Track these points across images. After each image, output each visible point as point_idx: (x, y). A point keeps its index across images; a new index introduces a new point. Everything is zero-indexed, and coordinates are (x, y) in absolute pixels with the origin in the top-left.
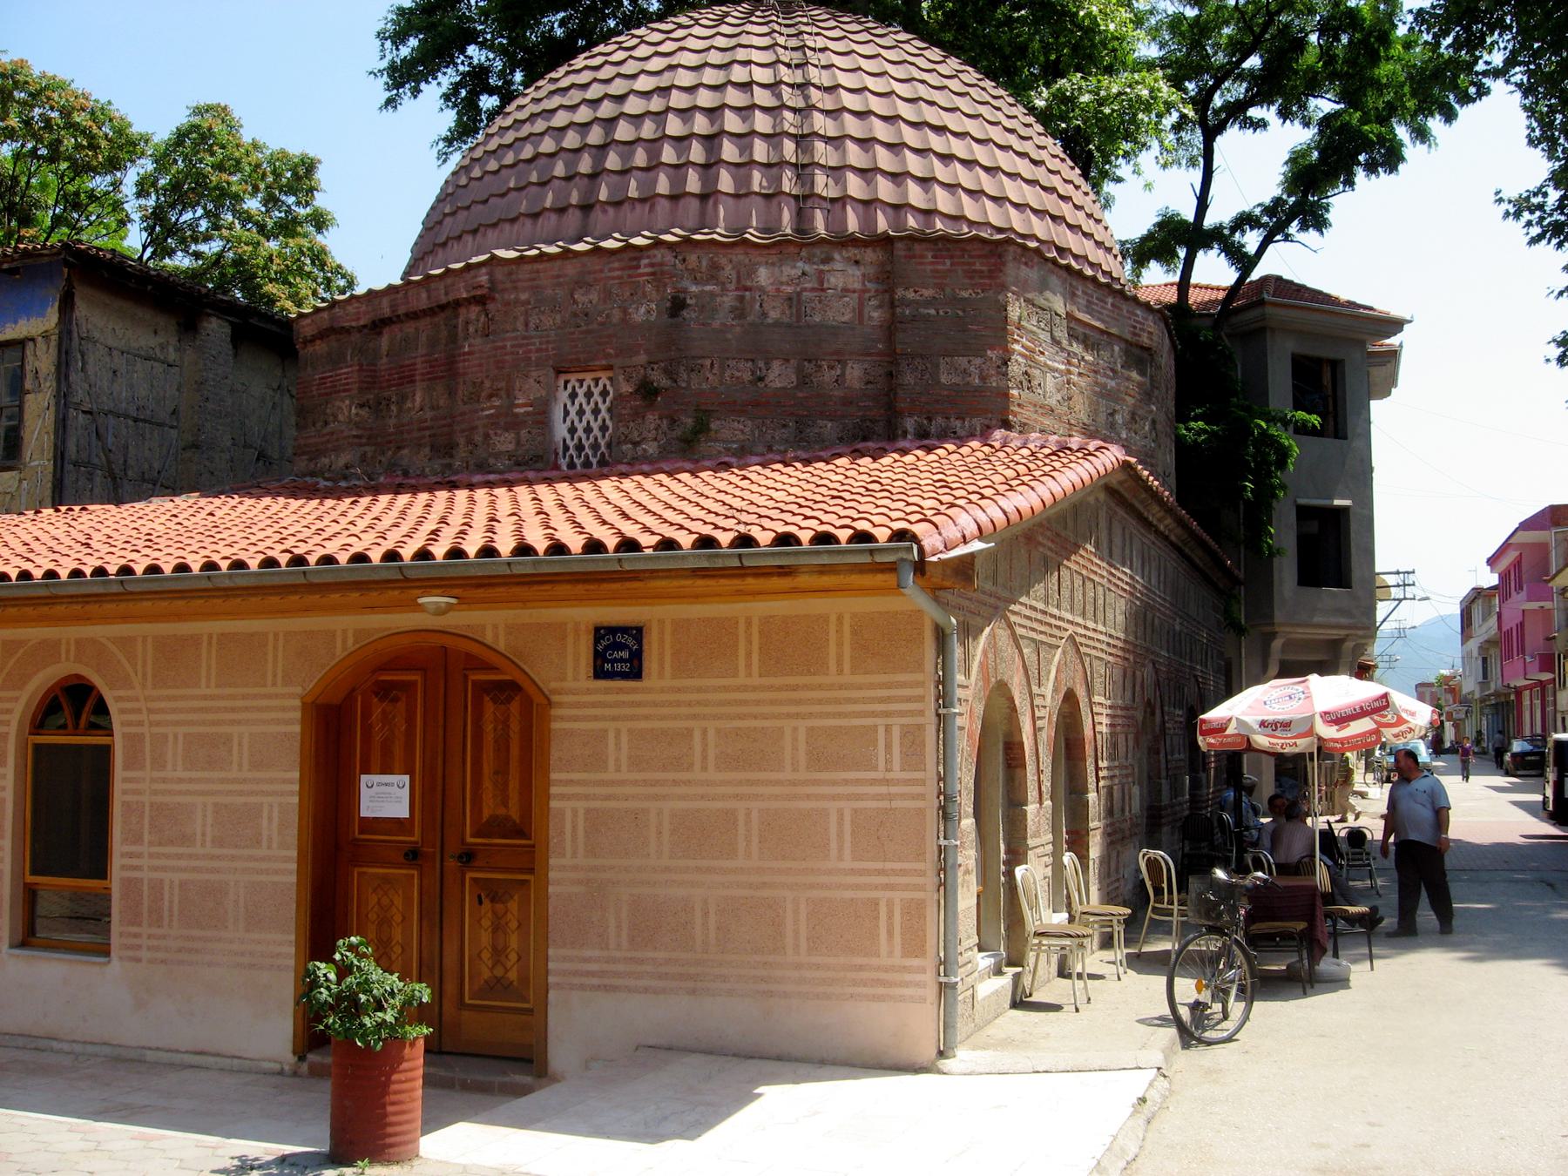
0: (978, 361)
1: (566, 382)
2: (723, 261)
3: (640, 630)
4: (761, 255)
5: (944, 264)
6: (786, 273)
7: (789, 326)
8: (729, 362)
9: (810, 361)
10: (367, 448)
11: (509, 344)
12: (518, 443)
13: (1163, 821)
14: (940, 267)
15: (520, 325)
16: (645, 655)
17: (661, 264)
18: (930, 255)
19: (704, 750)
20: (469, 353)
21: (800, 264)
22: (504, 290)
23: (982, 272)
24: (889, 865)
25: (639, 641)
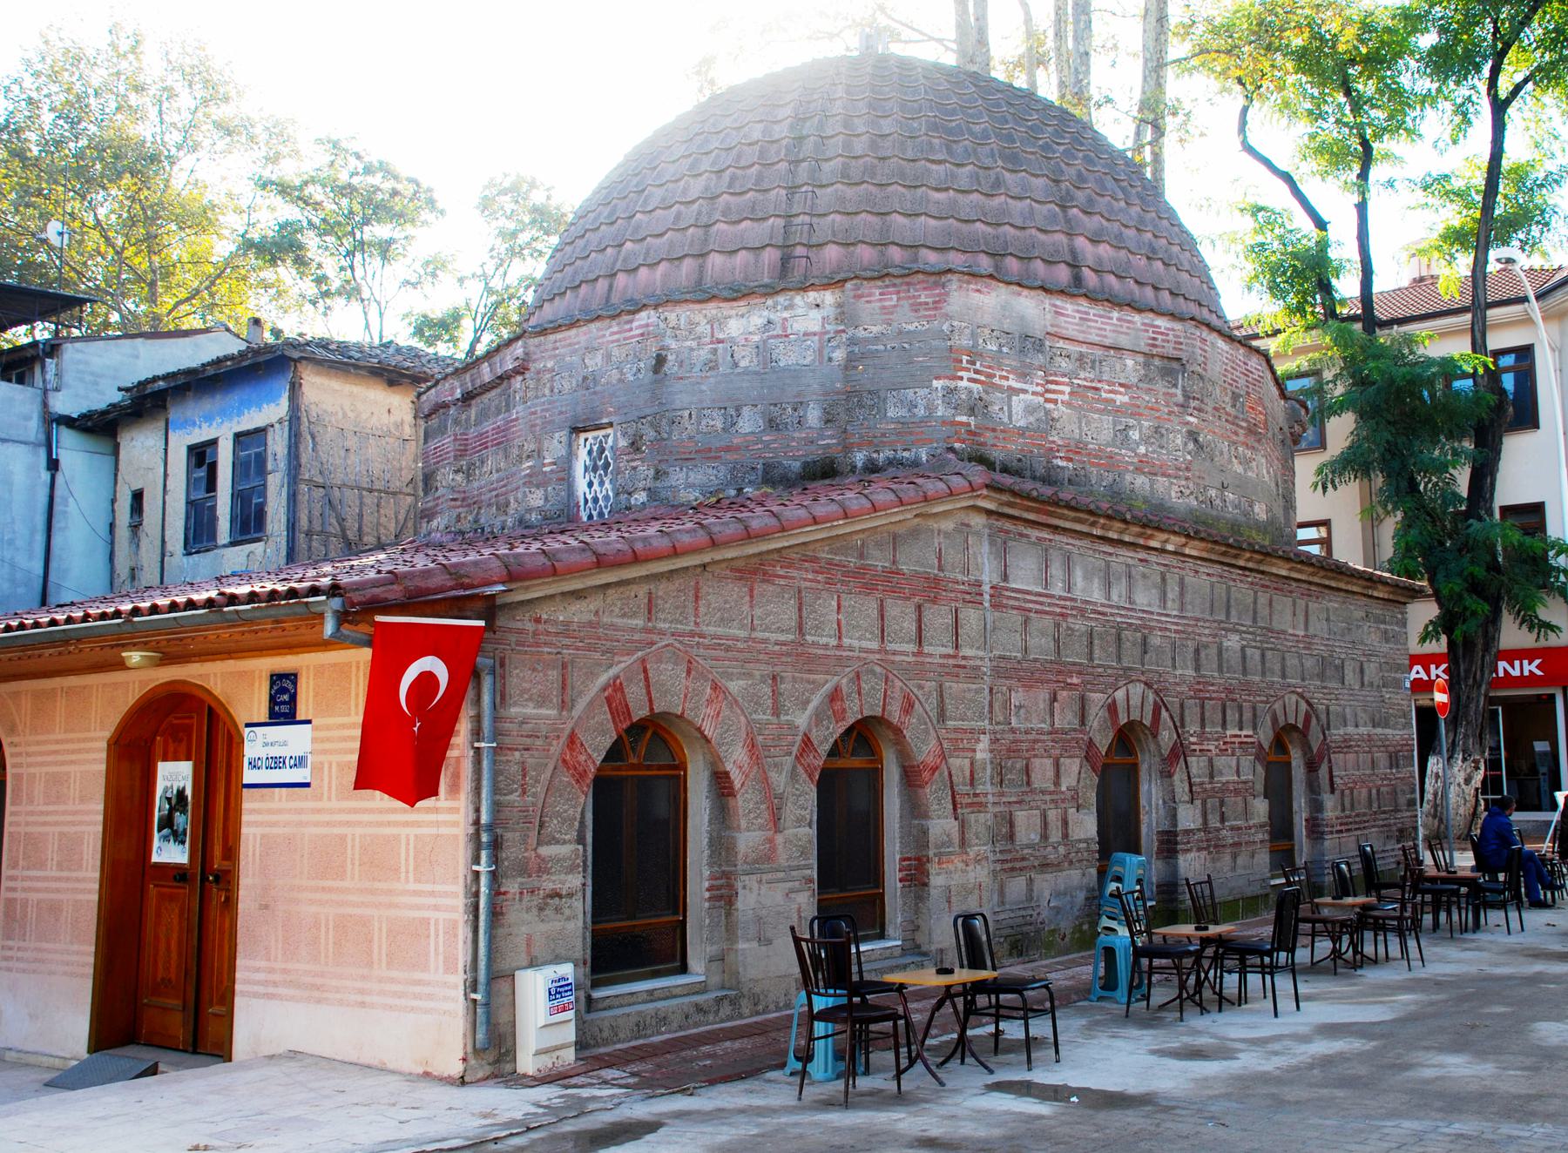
0: (922, 392)
1: (586, 440)
2: (698, 318)
3: (296, 675)
4: (732, 308)
5: (891, 299)
6: (752, 323)
7: (757, 373)
8: (705, 412)
9: (776, 405)
10: (461, 510)
11: (539, 409)
12: (546, 499)
13: (1179, 847)
14: (887, 304)
15: (547, 391)
16: (298, 697)
17: (647, 325)
18: (877, 292)
19: (330, 783)
20: (517, 419)
21: (766, 313)
22: (535, 361)
23: (927, 303)
24: (438, 888)
25: (295, 683)
